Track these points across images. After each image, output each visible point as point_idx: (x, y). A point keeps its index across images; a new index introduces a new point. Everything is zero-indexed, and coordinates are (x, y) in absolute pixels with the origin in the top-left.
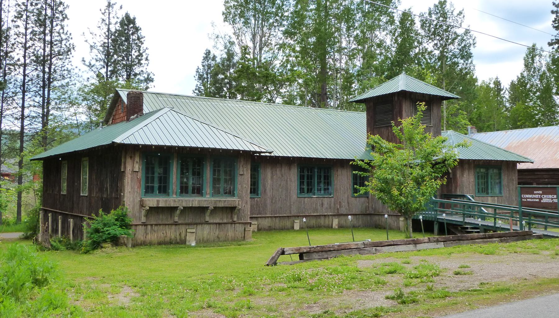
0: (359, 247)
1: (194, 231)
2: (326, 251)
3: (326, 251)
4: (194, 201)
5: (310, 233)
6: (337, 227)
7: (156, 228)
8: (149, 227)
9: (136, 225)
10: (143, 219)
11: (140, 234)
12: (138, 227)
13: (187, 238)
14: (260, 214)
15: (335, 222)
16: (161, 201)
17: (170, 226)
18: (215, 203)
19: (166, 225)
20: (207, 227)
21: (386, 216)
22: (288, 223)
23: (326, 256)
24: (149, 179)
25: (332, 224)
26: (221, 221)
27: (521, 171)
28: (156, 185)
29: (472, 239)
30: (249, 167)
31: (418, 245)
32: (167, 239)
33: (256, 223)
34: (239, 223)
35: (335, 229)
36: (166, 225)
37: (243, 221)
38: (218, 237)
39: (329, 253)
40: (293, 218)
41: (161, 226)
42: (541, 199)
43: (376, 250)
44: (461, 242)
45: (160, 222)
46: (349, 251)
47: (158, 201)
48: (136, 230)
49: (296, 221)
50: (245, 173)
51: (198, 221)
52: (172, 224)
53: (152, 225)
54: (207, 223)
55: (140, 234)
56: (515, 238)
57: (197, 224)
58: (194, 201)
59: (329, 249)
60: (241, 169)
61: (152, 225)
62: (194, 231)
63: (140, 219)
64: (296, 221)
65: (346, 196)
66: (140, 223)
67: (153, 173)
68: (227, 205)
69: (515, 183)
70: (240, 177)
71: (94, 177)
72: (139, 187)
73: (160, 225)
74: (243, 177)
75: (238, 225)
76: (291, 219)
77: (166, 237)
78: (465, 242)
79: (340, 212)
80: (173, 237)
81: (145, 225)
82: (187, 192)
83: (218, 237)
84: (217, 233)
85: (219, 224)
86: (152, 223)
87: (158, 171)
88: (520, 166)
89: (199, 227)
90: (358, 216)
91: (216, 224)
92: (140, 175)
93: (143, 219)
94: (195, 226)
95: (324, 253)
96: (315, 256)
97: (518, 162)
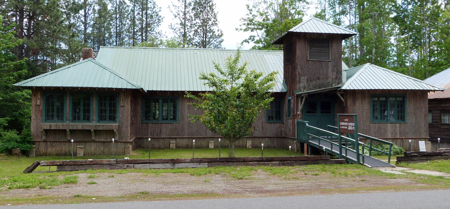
0: (111, 163)
1: (82, 146)
2: (78, 165)
3: (78, 165)
4: (79, 125)
5: (151, 152)
6: (250, 147)
7: (54, 144)
8: (49, 143)
9: (39, 142)
10: (44, 138)
11: (42, 148)
12: (40, 143)
13: (78, 152)
14: (179, 135)
15: (249, 143)
16: (54, 125)
17: (65, 143)
18: (95, 127)
19: (61, 142)
20: (94, 145)
21: (72, 141)
22: (204, 143)
23: (77, 169)
24: (47, 111)
25: (246, 145)
26: (105, 140)
27: (430, 100)
28: (108, 114)
29: (244, 161)
30: (129, 100)
31: (176, 164)
32: (63, 152)
33: (213, 142)
34: (121, 142)
35: (249, 149)
36: (61, 142)
37: (123, 141)
38: (103, 152)
39: (81, 166)
40: (209, 139)
41: (58, 143)
42: (348, 126)
43: (127, 166)
44: (231, 163)
45: (57, 140)
46: (101, 166)
47: (50, 126)
48: (39, 145)
49: (210, 141)
50: (126, 105)
51: (86, 140)
52: (66, 142)
53: (50, 142)
54: (94, 141)
55: (42, 148)
56: (302, 162)
57: (85, 142)
58: (79, 125)
59: (82, 164)
60: (122, 102)
61: (50, 142)
62: (82, 146)
63: (42, 138)
64: (210, 141)
65: (260, 122)
66: (42, 140)
67: (53, 106)
68: (105, 128)
69: (424, 110)
70: (121, 108)
71: (139, 109)
72: (41, 116)
73: (57, 142)
74: (123, 108)
75: (119, 143)
76: (207, 140)
77: (62, 150)
78: (235, 163)
79: (254, 135)
80: (67, 151)
81: (45, 142)
82: (79, 119)
83: (103, 152)
84: (102, 149)
85: (104, 142)
86: (51, 140)
87: (57, 104)
88: (431, 96)
89: (88, 144)
90: (272, 139)
91: (101, 142)
92: (41, 108)
93: (44, 138)
94: (84, 143)
95: (76, 166)
96: (67, 168)
97: (429, 91)
